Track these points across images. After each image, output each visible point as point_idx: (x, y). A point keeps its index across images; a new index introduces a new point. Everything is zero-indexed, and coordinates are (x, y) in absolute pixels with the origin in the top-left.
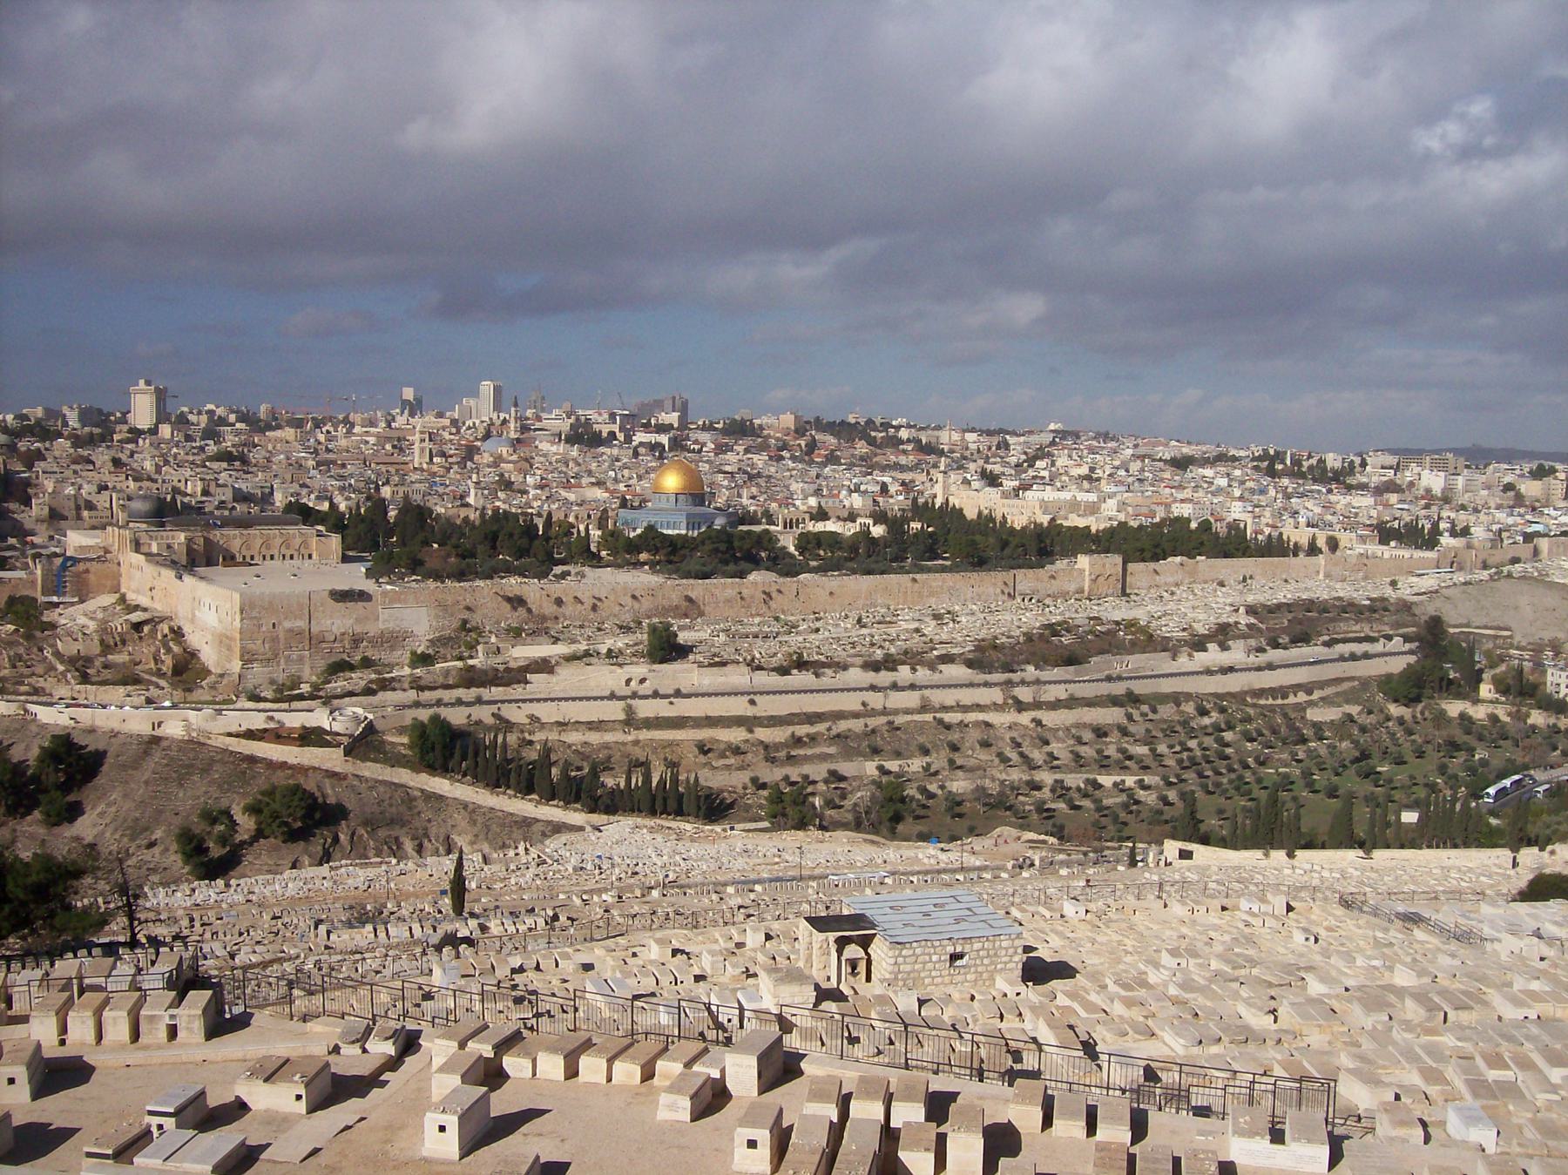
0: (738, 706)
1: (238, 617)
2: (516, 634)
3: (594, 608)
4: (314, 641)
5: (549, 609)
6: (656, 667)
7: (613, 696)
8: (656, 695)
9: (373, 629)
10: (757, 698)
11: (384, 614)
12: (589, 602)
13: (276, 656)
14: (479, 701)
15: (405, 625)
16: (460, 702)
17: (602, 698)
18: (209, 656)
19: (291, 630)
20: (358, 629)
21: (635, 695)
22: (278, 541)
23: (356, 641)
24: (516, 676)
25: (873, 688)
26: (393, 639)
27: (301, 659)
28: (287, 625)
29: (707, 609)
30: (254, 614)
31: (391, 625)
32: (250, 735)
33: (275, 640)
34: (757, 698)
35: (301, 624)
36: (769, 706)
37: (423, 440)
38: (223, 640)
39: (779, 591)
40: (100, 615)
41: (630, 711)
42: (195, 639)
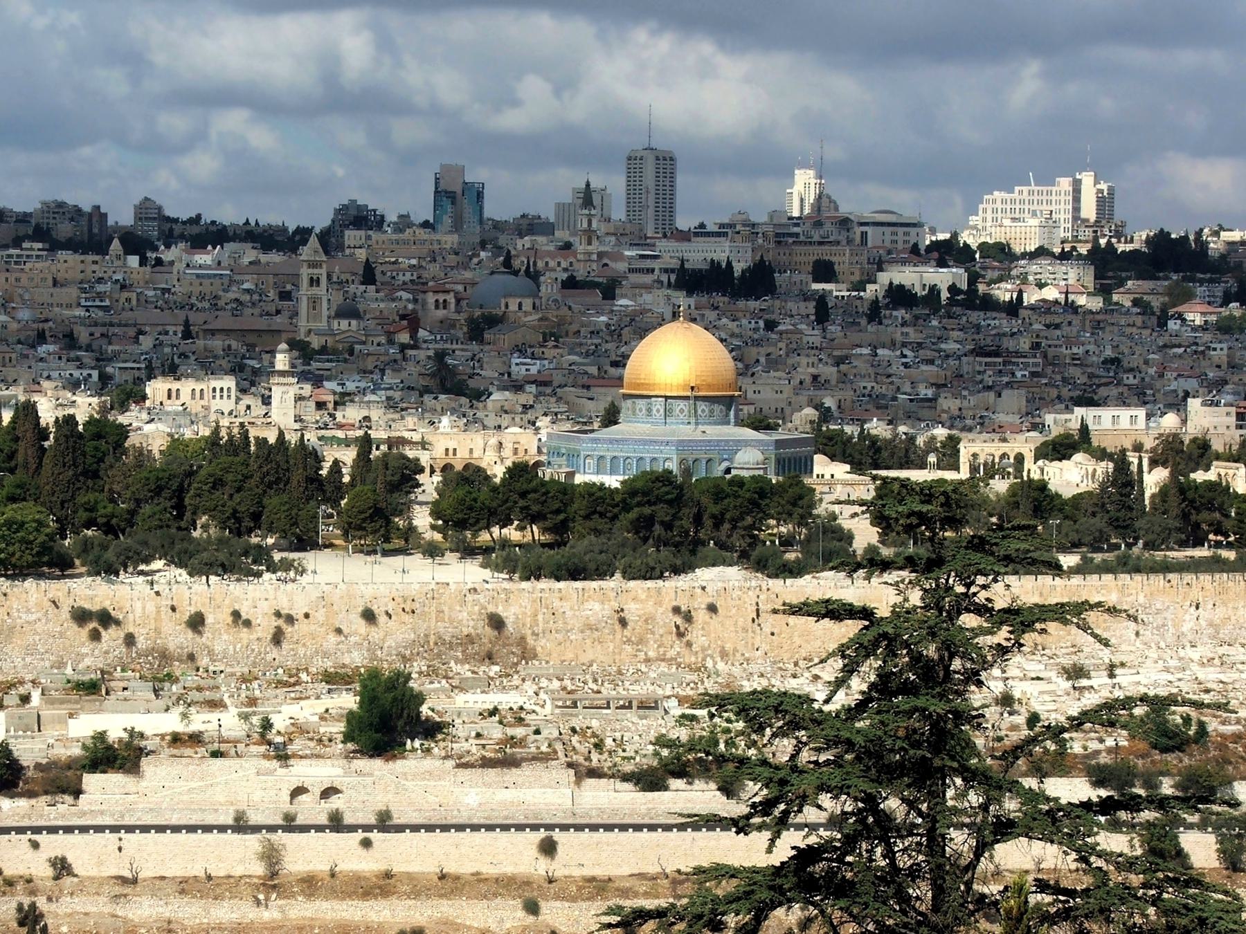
0: (517, 855)
2: (91, 689)
3: (277, 638)
5: (178, 638)
6: (362, 763)
7: (241, 826)
8: (337, 824)
10: (557, 835)
12: (265, 625)
17: (222, 829)
21: (290, 825)
24: (62, 781)
29: (542, 645)
34: (557, 835)
36: (581, 856)
37: (314, 282)
39: (712, 608)
41: (271, 857)
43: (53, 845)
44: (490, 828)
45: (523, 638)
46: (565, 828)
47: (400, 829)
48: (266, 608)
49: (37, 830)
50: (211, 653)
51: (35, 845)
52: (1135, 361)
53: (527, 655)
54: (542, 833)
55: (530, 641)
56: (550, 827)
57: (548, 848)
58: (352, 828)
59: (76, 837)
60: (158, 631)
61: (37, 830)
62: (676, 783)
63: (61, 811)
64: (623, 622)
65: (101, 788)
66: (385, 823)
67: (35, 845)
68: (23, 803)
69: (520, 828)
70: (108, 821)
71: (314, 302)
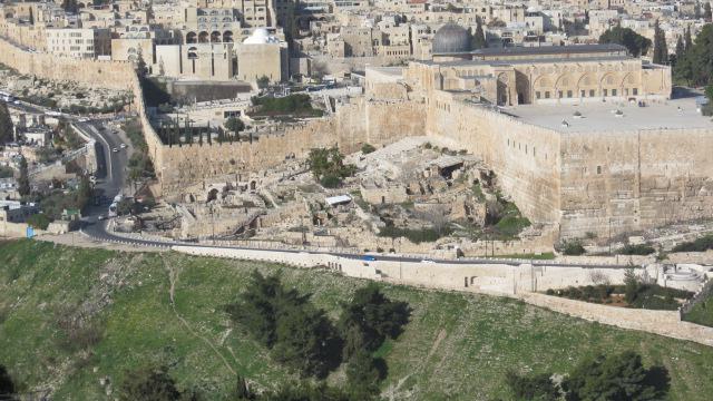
1: (559, 157)
4: (647, 188)
18: (524, 203)
20: (696, 174)
22: (599, 75)
27: (630, 208)
28: (614, 169)
32: (573, 293)
33: (601, 186)
35: (629, 167)
38: (540, 186)
40: (404, 160)
42: (510, 186)
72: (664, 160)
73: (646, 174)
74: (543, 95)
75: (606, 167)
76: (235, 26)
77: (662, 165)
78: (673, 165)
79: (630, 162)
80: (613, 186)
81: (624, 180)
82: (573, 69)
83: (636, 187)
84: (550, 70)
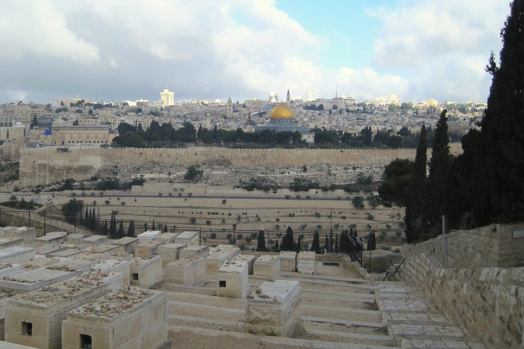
4: (52, 170)
5: (156, 159)
8: (180, 196)
9: (76, 165)
10: (227, 199)
11: (81, 159)
13: (35, 174)
14: (101, 195)
15: (90, 164)
16: (93, 195)
17: (157, 197)
19: (40, 164)
22: (92, 135)
23: (69, 169)
24: (128, 186)
25: (287, 197)
26: (85, 169)
28: (39, 162)
29: (233, 162)
30: (25, 157)
31: (85, 164)
33: (34, 168)
34: (227, 199)
35: (44, 162)
43: (122, 200)
44: (213, 197)
45: (229, 161)
46: (229, 198)
47: (194, 197)
48: (175, 153)
49: (120, 196)
50: (163, 162)
51: (118, 199)
52: (391, 121)
53: (230, 163)
54: (223, 199)
55: (231, 161)
56: (226, 198)
57: (224, 202)
58: (184, 197)
59: (128, 198)
60: (152, 158)
61: (120, 196)
62: (255, 189)
63: (127, 193)
64: (251, 157)
65: (136, 189)
66: (190, 195)
67: (118, 199)
68: (120, 191)
69: (219, 197)
70: (136, 195)
71: (230, 110)
72: (58, 159)
73: (51, 164)
74: (71, 142)
75: (36, 161)
76: (14, 121)
77: (57, 161)
78: (61, 161)
79: (45, 160)
80: (39, 169)
81: (43, 166)
82: (82, 133)
83: (48, 169)
84: (74, 133)
